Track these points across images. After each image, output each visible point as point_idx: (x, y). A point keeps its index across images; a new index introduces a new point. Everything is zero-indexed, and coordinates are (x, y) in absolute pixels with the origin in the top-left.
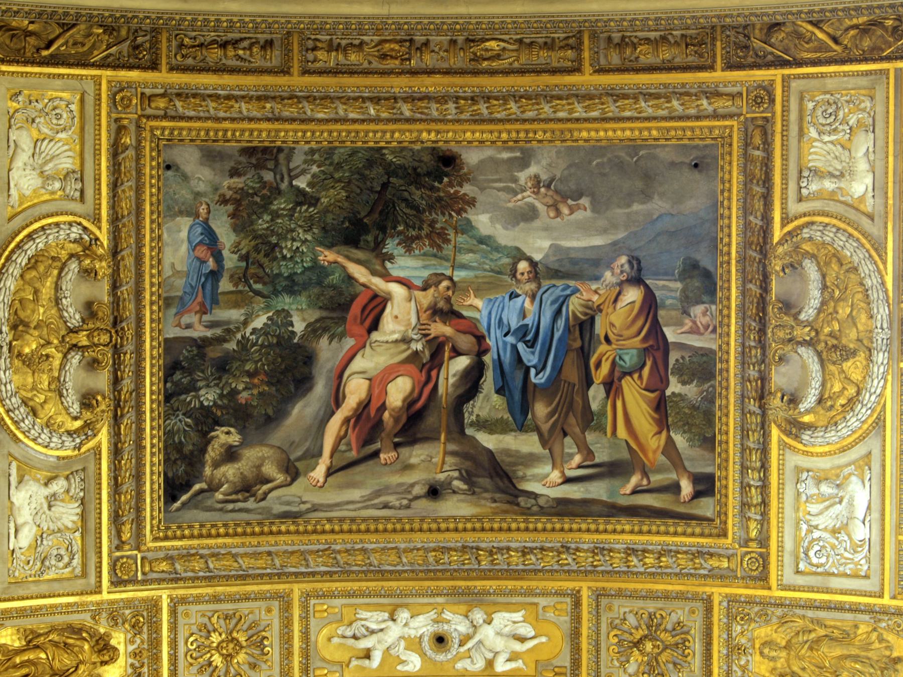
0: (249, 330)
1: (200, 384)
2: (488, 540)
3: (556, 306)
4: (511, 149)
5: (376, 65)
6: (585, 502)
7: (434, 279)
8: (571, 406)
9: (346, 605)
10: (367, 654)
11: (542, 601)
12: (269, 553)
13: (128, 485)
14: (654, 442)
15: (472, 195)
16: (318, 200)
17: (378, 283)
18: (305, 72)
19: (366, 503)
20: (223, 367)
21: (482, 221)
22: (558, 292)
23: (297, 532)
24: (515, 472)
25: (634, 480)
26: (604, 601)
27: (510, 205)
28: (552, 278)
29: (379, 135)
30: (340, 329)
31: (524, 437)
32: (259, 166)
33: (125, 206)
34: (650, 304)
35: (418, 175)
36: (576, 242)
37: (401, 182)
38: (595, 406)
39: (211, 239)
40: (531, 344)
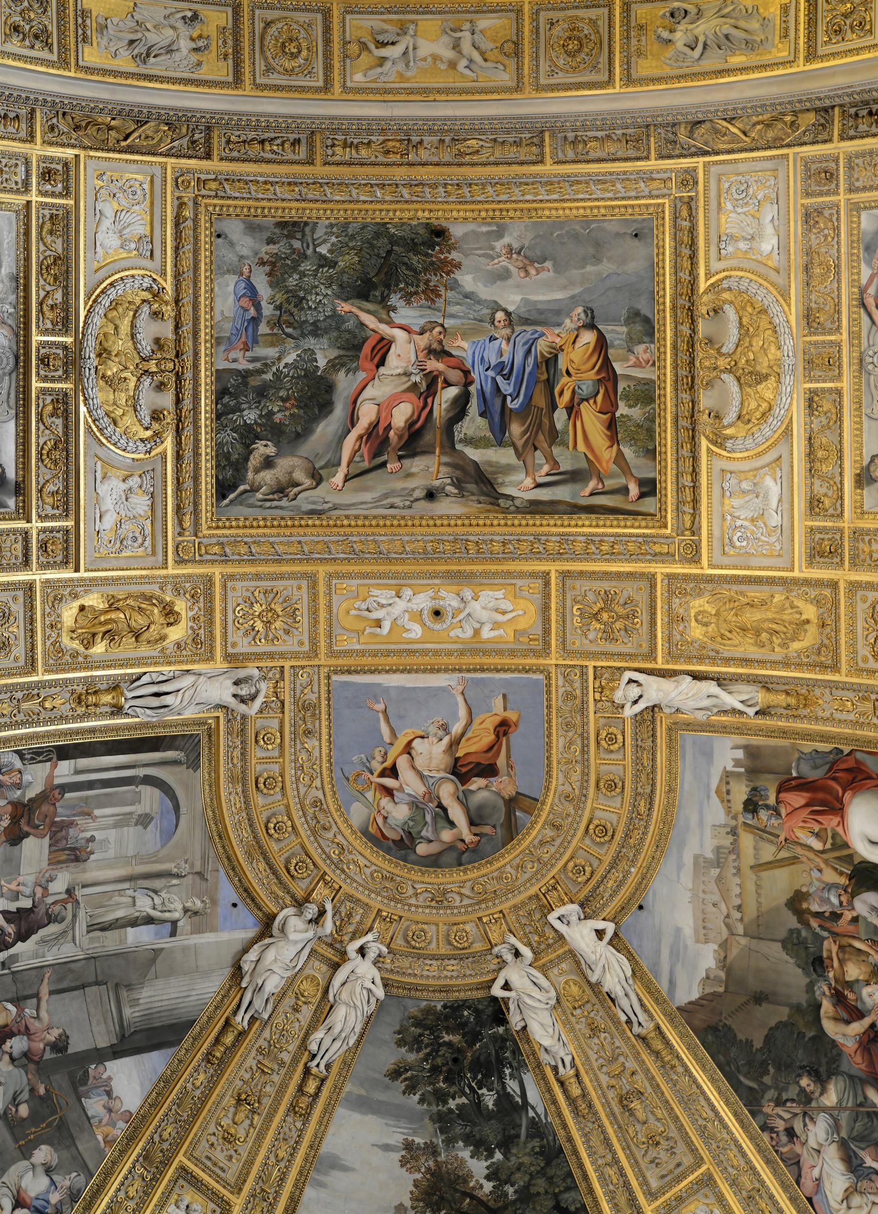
0: (282, 365)
1: (244, 406)
2: (474, 533)
3: (527, 347)
4: (489, 224)
5: (381, 159)
6: (552, 503)
7: (429, 326)
8: (540, 426)
9: (361, 585)
10: (378, 623)
11: (519, 582)
12: (300, 542)
15: (458, 260)
16: (336, 263)
18: (326, 163)
22: (528, 336)
23: (321, 526)
24: (495, 479)
26: (568, 582)
27: (489, 268)
28: (523, 324)
29: (383, 213)
30: (354, 365)
31: (502, 451)
35: (416, 244)
36: (542, 297)
37: (402, 250)
38: (559, 426)
39: (252, 292)
40: (507, 377)
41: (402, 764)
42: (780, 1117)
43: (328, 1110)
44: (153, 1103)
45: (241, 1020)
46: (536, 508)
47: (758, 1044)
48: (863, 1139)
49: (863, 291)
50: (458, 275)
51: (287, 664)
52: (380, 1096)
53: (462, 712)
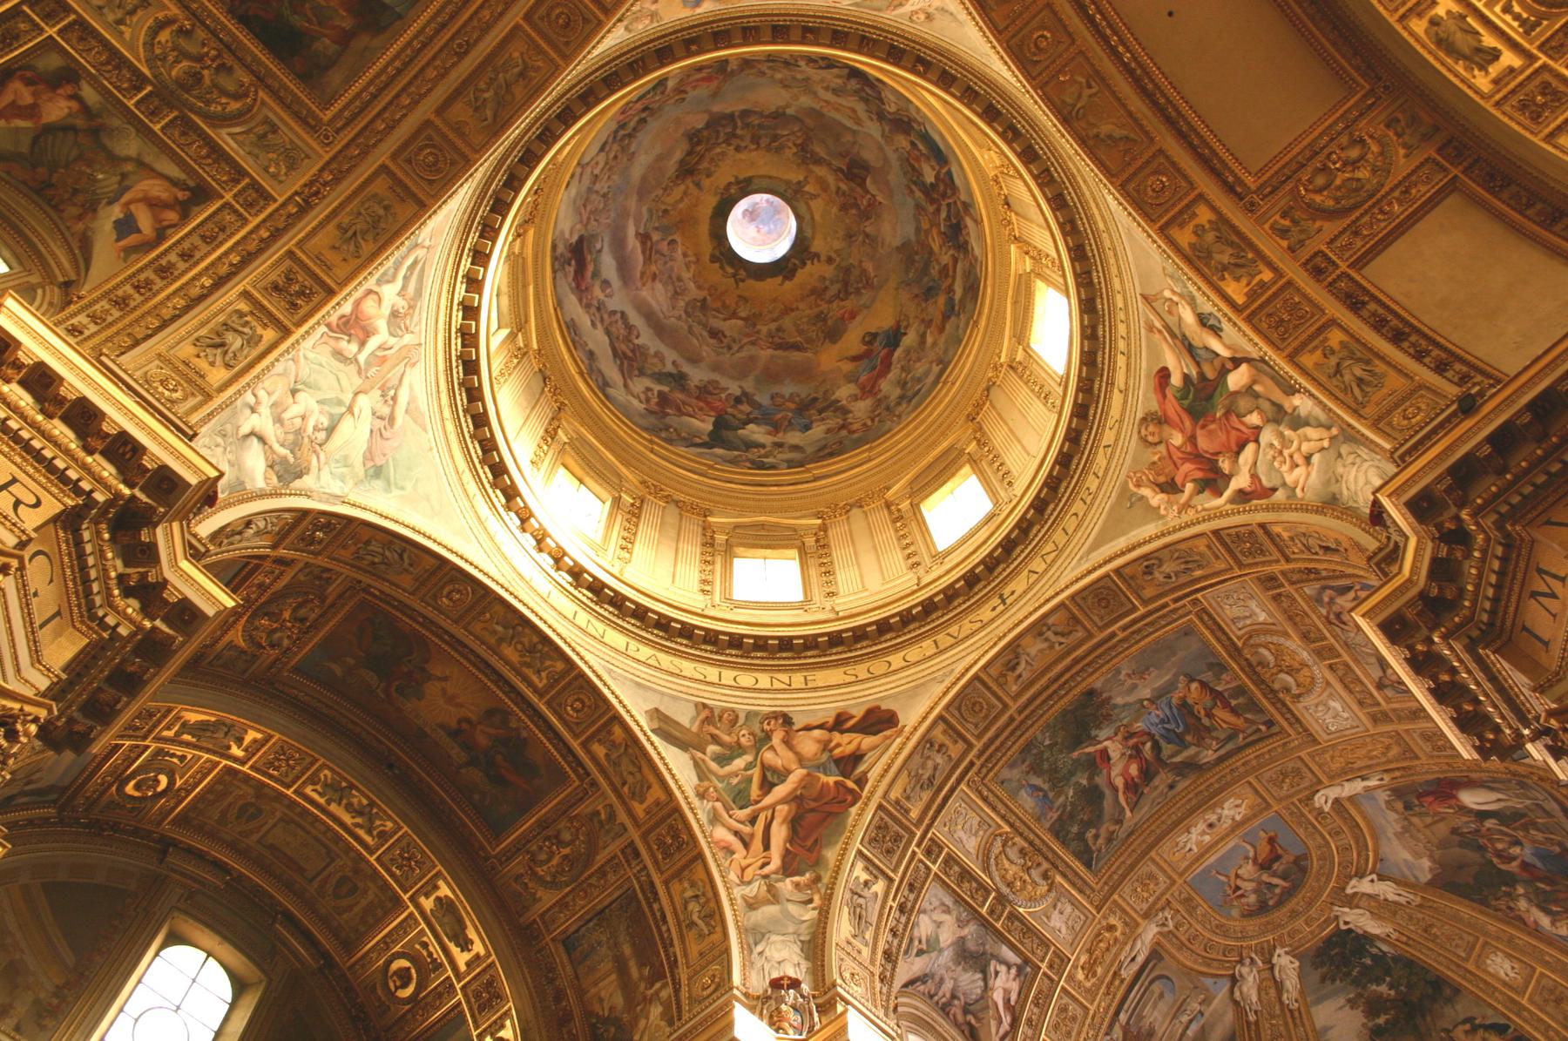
13: (1076, 880)
14: (1240, 722)
17: (1099, 747)
20: (1072, 816)
21: (1119, 700)
34: (1203, 685)
41: (1239, 882)
42: (1502, 904)
43: (1309, 1013)
45: (1252, 1018)
46: (1221, 760)
49: (1327, 618)
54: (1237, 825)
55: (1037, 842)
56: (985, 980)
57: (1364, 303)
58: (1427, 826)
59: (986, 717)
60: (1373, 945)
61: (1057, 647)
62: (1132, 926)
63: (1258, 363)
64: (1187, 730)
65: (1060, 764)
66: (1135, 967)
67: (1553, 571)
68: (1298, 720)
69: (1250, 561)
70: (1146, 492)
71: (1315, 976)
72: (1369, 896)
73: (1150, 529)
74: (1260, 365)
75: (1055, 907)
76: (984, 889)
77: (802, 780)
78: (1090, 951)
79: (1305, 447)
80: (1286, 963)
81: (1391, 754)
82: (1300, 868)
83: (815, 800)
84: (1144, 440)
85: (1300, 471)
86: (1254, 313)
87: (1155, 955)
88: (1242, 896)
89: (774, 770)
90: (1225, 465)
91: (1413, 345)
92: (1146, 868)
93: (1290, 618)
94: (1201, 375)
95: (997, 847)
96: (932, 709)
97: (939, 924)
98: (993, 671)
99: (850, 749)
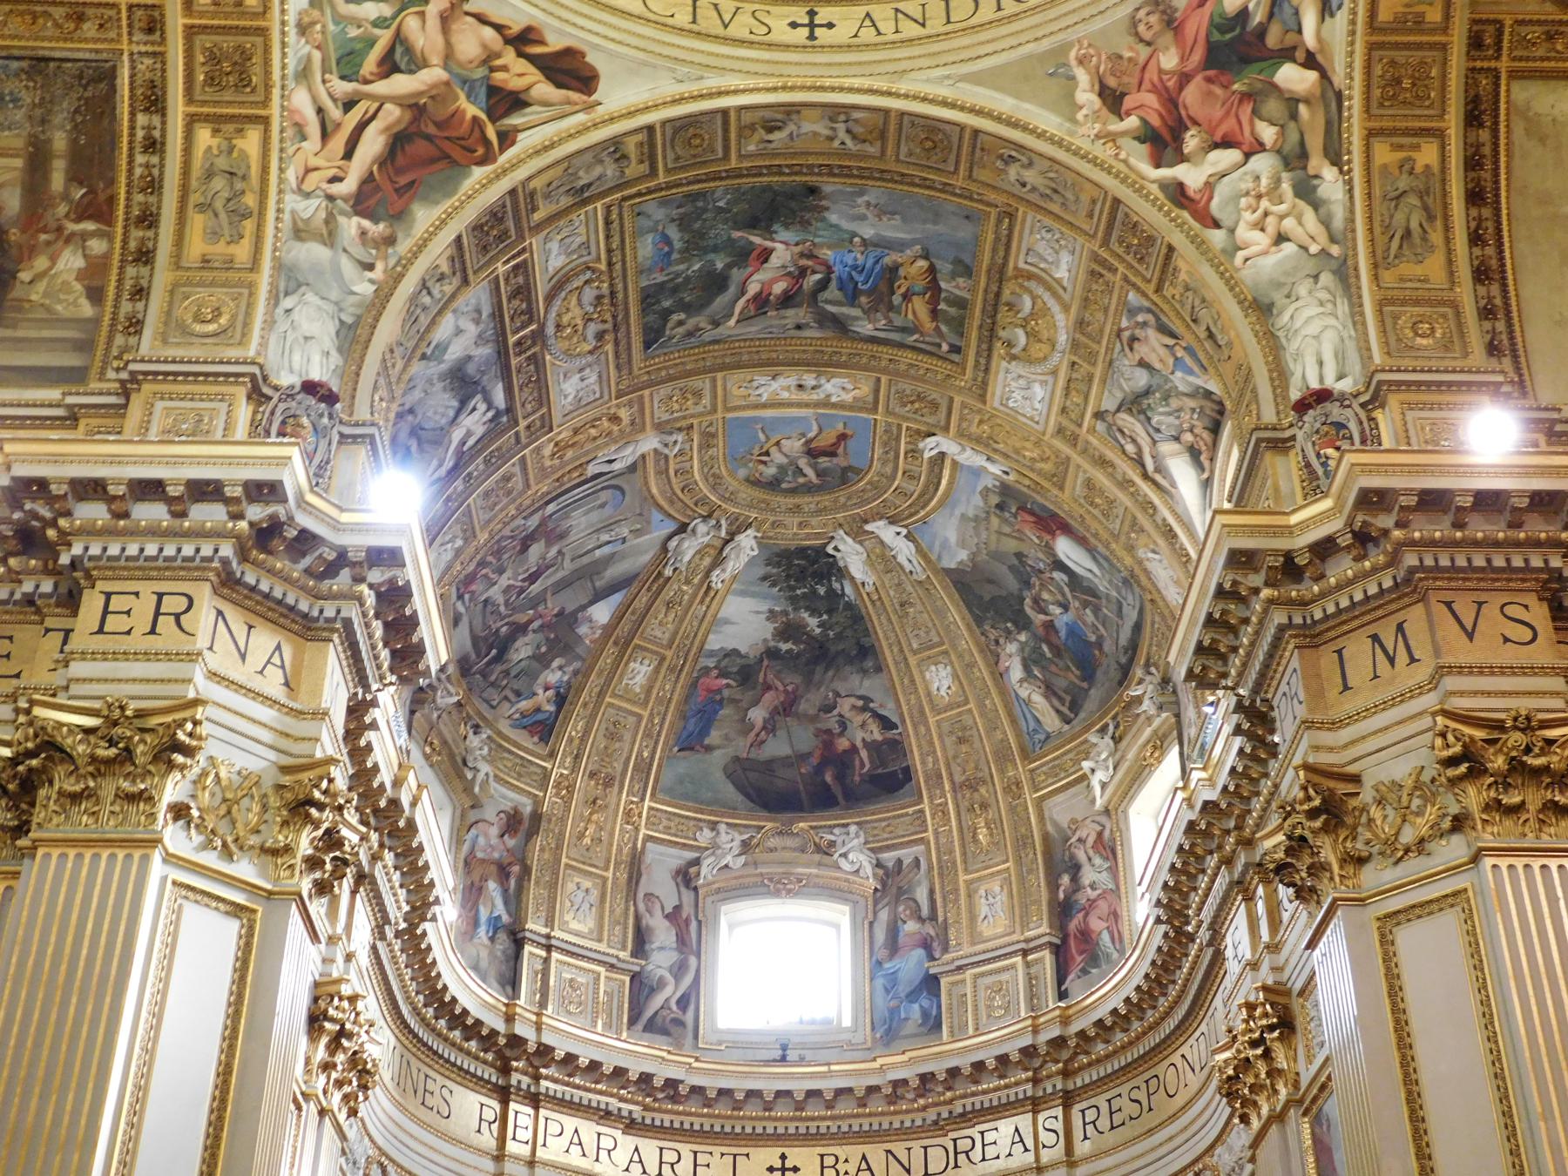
13: (624, 356)
17: (768, 244)
19: (759, 332)
20: (675, 290)
21: (833, 218)
25: (916, 337)
32: (694, 201)
33: (615, 244)
34: (932, 270)
36: (889, 234)
41: (773, 450)
44: (618, 617)
45: (668, 572)
46: (873, 340)
47: (987, 597)
48: (1036, 662)
50: (826, 214)
51: (695, 422)
52: (757, 589)
53: (815, 428)
54: (826, 403)
55: (620, 296)
56: (458, 412)
57: (1481, 125)
58: (999, 533)
59: (694, 156)
60: (839, 580)
61: (836, 144)
62: (637, 426)
63: (1331, 97)
64: (869, 293)
65: (712, 233)
66: (605, 468)
67: (1412, 643)
68: (987, 370)
69: (1120, 251)
70: (1083, 77)
71: (761, 571)
72: (882, 542)
73: (1049, 121)
74: (1331, 94)
75: (581, 370)
76: (530, 314)
77: (434, 86)
78: (576, 432)
79: (1289, 224)
80: (747, 542)
81: (1039, 465)
82: (846, 476)
83: (438, 125)
84: (1134, 23)
85: (1261, 240)
86: (1381, 46)
87: (632, 468)
88: (764, 463)
89: (409, 50)
90: (1191, 141)
91: (1480, 220)
92: (702, 383)
93: (1086, 299)
94: (1262, 32)
95: (577, 283)
96: (647, 109)
97: (459, 332)
98: (747, 118)
99: (515, 84)
